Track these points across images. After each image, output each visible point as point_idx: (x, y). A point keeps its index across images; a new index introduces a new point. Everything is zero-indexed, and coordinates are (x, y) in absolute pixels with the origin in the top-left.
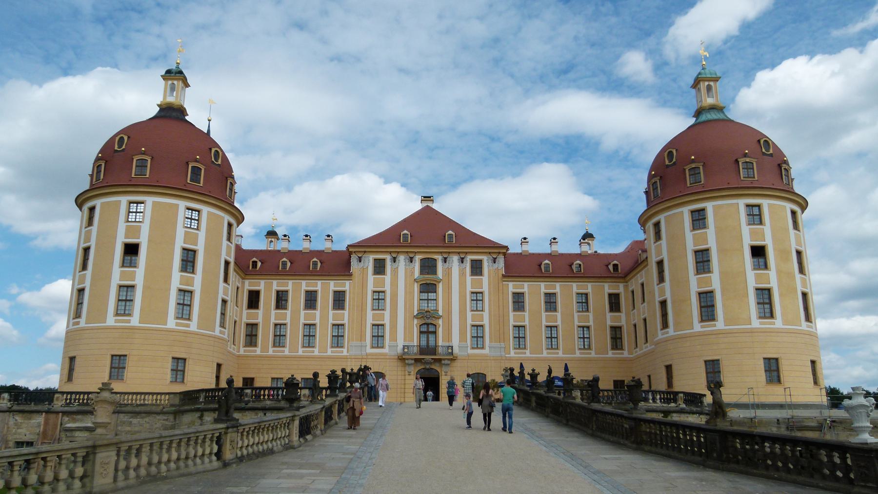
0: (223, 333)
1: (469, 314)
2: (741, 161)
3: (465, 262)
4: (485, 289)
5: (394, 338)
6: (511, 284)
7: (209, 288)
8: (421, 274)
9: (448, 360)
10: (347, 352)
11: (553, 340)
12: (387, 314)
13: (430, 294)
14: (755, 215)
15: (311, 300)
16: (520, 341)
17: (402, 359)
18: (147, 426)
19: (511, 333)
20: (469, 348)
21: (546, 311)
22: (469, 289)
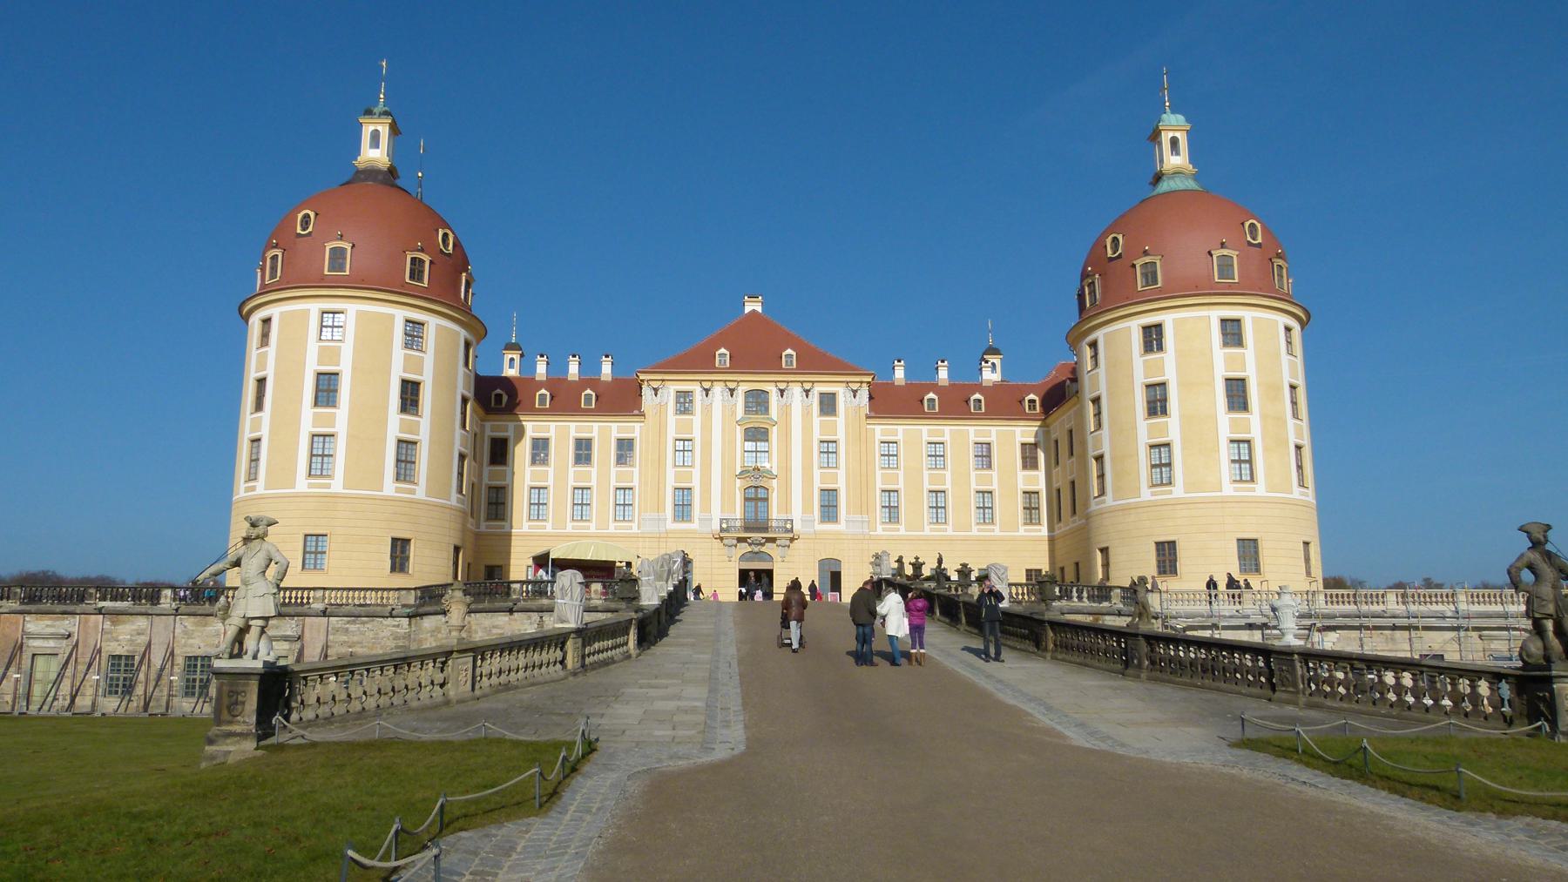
1: (817, 473)
2: (1216, 254)
3: (810, 396)
4: (841, 436)
5: (706, 507)
6: (878, 429)
11: (939, 510)
12: (696, 473)
13: (759, 444)
14: (1232, 332)
15: (583, 452)
16: (892, 512)
18: (371, 635)
20: (816, 522)
22: (817, 436)
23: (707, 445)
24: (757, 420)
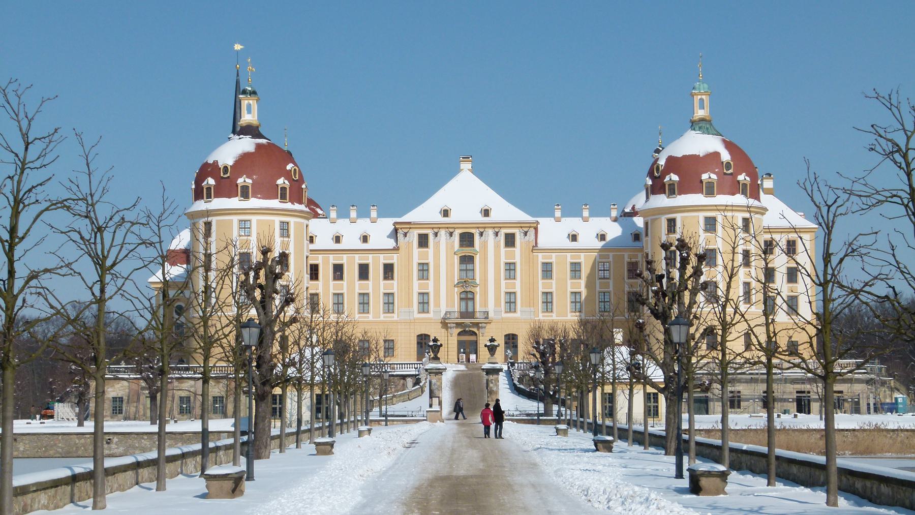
1: (503, 282)
3: (499, 235)
4: (517, 260)
5: (437, 304)
8: (460, 247)
9: (485, 323)
10: (398, 317)
17: (445, 324)
19: (540, 299)
20: (503, 312)
21: (572, 278)
22: (503, 260)
23: (437, 267)
24: (467, 251)
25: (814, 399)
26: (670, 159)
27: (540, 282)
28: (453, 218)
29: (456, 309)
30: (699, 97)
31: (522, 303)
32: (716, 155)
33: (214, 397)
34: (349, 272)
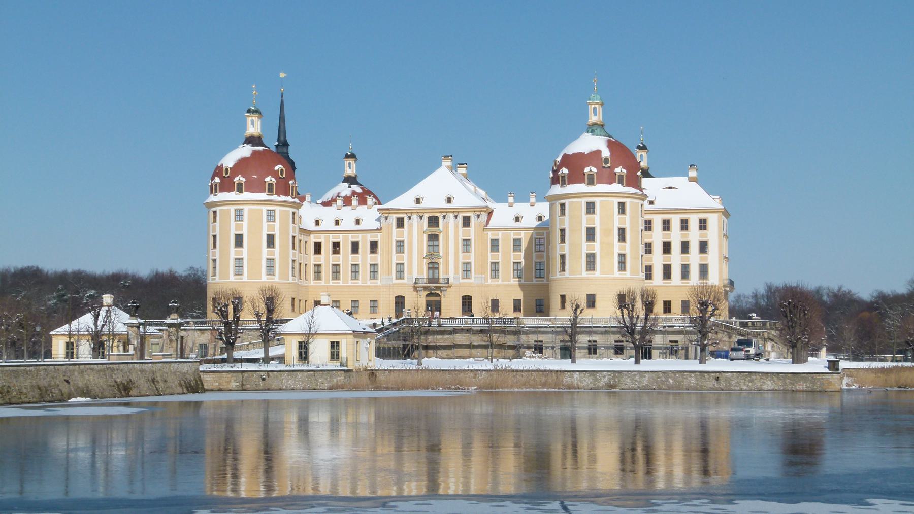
0: (295, 280)
1: (461, 255)
4: (472, 237)
5: (410, 272)
7: (284, 255)
9: (445, 287)
20: (460, 279)
22: (461, 237)
23: (410, 244)
24: (433, 231)
25: (654, 347)
26: (566, 157)
27: (490, 254)
28: (423, 205)
29: (425, 276)
30: (593, 106)
31: (475, 271)
32: (598, 152)
33: (200, 344)
34: (346, 248)
